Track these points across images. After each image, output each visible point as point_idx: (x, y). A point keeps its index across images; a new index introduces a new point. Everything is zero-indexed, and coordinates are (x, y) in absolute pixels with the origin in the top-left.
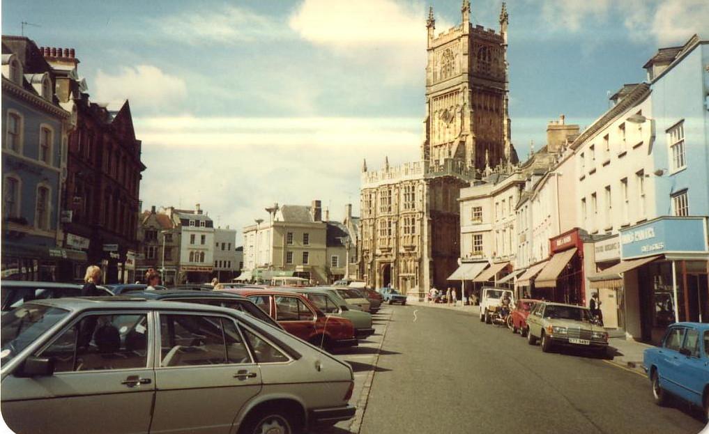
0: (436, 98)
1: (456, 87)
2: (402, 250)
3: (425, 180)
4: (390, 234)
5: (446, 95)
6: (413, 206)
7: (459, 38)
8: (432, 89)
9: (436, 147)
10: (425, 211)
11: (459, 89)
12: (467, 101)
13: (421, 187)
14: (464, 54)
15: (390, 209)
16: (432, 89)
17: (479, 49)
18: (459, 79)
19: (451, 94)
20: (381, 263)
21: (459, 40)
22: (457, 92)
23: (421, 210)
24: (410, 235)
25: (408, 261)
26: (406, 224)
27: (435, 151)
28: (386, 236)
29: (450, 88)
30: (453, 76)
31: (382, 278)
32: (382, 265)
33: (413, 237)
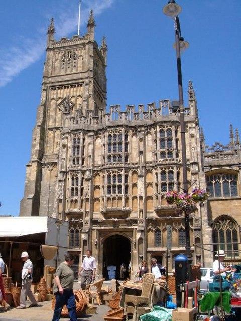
0: (53, 88)
1: (80, 81)
2: (154, 215)
4: (126, 192)
5: (66, 87)
7: (84, 44)
8: (50, 80)
9: (51, 129)
11: (84, 82)
12: (92, 93)
16: (50, 80)
18: (86, 75)
19: (73, 86)
22: (80, 85)
25: (164, 230)
27: (51, 134)
29: (72, 80)
30: (74, 71)
31: (102, 254)
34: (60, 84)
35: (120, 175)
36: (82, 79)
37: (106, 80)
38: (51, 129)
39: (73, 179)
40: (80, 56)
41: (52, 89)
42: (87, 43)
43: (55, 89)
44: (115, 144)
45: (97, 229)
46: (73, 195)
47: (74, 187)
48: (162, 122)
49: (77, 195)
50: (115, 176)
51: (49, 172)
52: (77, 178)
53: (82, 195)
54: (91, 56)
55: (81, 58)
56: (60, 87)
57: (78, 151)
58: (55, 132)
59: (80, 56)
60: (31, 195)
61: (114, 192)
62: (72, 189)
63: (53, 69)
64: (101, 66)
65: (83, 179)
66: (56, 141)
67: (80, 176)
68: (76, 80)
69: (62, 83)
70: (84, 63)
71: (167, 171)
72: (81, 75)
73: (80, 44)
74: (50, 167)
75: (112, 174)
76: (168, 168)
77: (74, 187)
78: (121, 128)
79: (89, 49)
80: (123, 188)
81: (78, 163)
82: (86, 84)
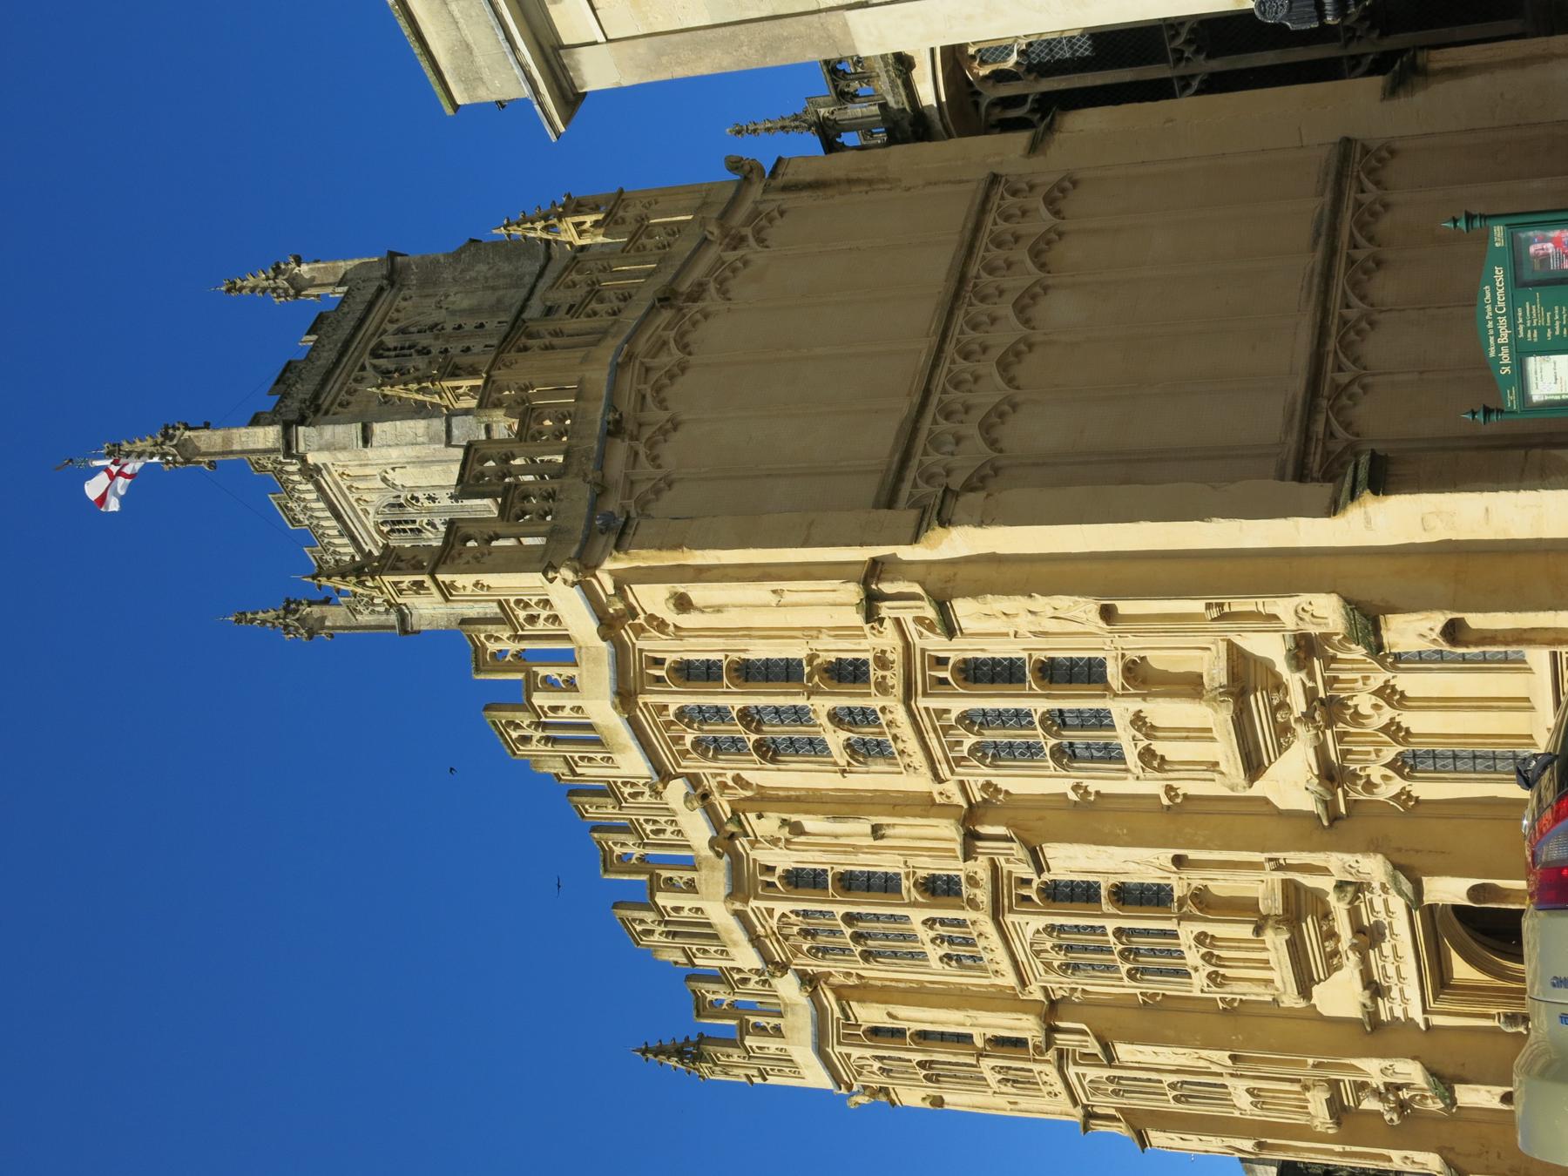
3: (585, 565)
6: (848, 673)
10: (863, 554)
13: (652, 598)
14: (366, 441)
15: (939, 888)
17: (370, 372)
20: (1440, 981)
21: (317, 469)
23: (852, 592)
24: (1121, 710)
25: (1394, 731)
26: (1032, 751)
28: (1187, 932)
32: (1462, 970)
33: (1139, 675)
40: (384, 480)
42: (303, 460)
45: (1425, 1011)
54: (366, 441)
55: (397, 477)
59: (384, 480)
70: (422, 463)
73: (319, 488)
75: (1058, 959)
79: (329, 447)
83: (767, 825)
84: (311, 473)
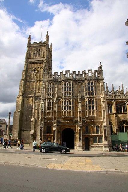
0: (30, 64)
5: (36, 63)
9: (29, 82)
19: (39, 63)
27: (27, 83)
34: (33, 62)
35: (70, 102)
36: (43, 60)
37: (52, 62)
38: (29, 82)
39: (48, 102)
41: (29, 64)
43: (31, 64)
44: (68, 88)
46: (48, 110)
47: (49, 106)
48: (89, 79)
49: (50, 110)
50: (68, 102)
51: (27, 100)
52: (50, 102)
53: (52, 110)
56: (33, 63)
57: (51, 90)
58: (30, 83)
60: (19, 110)
61: (68, 109)
62: (48, 107)
63: (30, 56)
64: (50, 56)
65: (53, 103)
66: (31, 87)
67: (51, 101)
68: (40, 60)
69: (34, 62)
71: (91, 100)
72: (42, 59)
74: (28, 98)
76: (92, 99)
77: (49, 106)
78: (70, 81)
80: (71, 107)
81: (50, 95)
82: (45, 63)
83: (80, 84)
84: (44, 46)
